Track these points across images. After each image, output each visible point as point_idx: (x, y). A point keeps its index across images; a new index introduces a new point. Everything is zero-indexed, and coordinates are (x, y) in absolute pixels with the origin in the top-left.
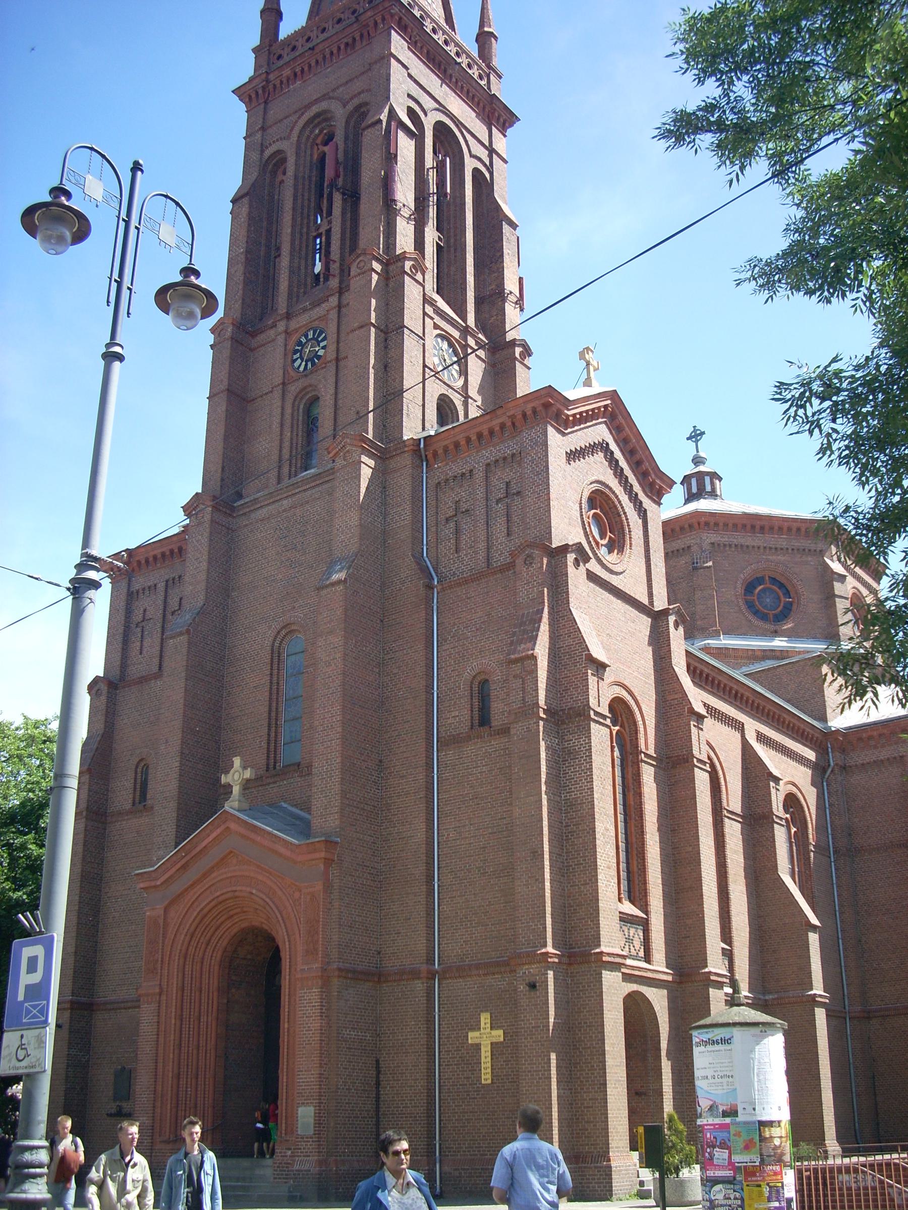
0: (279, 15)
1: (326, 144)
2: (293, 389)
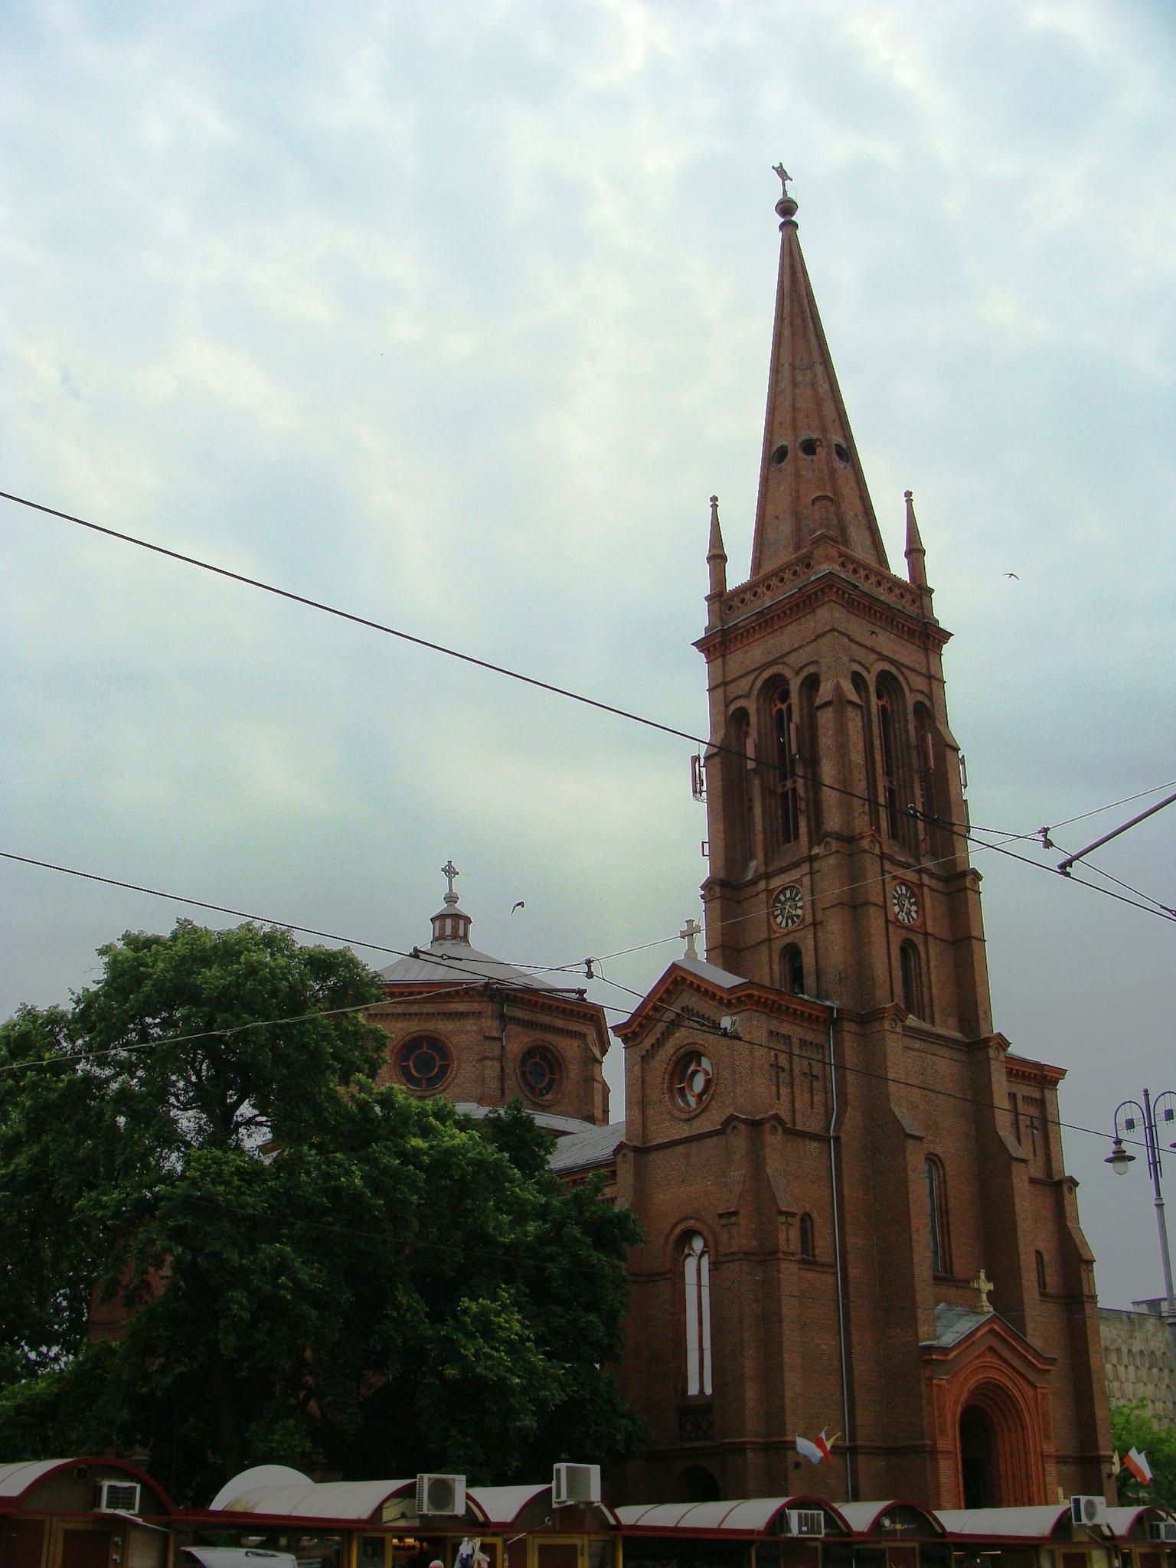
0: (724, 558)
1: (783, 702)
2: (777, 946)
